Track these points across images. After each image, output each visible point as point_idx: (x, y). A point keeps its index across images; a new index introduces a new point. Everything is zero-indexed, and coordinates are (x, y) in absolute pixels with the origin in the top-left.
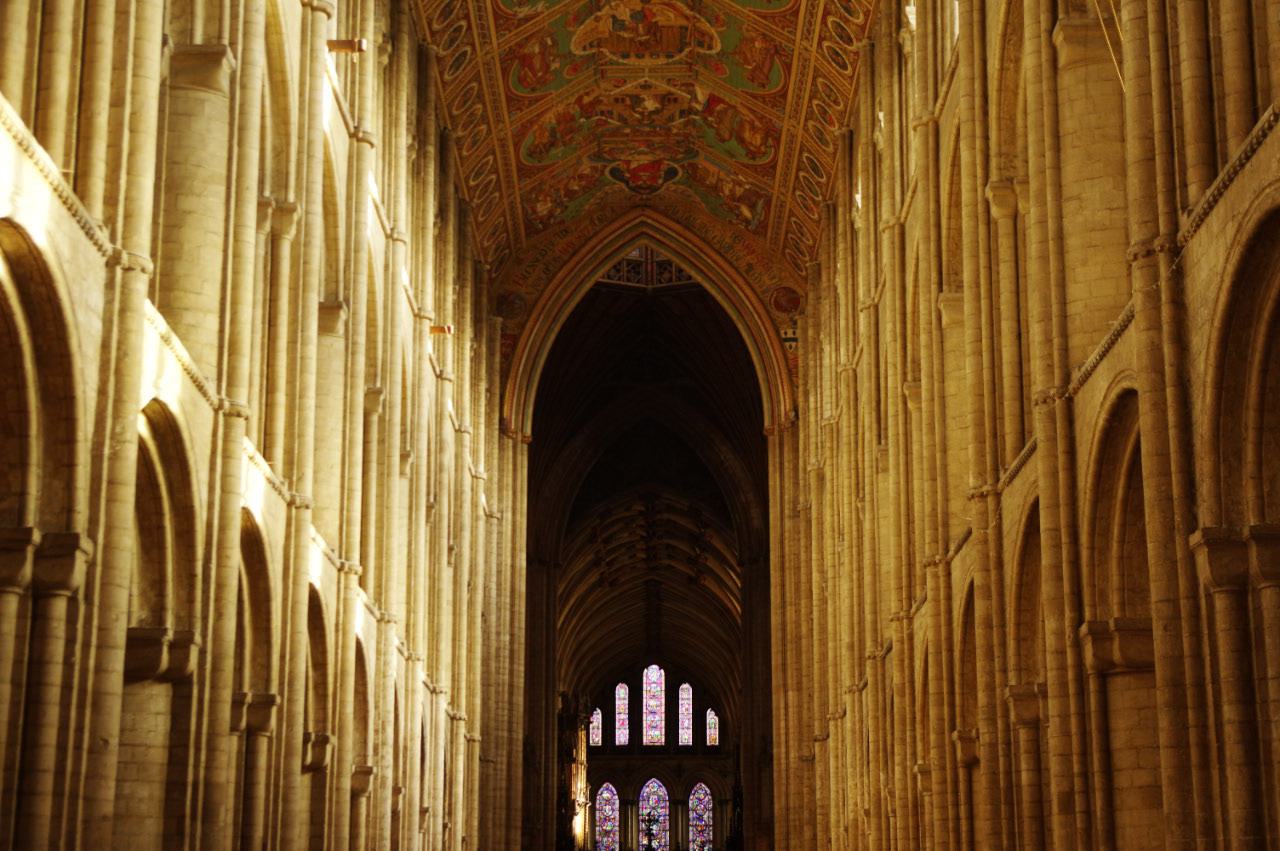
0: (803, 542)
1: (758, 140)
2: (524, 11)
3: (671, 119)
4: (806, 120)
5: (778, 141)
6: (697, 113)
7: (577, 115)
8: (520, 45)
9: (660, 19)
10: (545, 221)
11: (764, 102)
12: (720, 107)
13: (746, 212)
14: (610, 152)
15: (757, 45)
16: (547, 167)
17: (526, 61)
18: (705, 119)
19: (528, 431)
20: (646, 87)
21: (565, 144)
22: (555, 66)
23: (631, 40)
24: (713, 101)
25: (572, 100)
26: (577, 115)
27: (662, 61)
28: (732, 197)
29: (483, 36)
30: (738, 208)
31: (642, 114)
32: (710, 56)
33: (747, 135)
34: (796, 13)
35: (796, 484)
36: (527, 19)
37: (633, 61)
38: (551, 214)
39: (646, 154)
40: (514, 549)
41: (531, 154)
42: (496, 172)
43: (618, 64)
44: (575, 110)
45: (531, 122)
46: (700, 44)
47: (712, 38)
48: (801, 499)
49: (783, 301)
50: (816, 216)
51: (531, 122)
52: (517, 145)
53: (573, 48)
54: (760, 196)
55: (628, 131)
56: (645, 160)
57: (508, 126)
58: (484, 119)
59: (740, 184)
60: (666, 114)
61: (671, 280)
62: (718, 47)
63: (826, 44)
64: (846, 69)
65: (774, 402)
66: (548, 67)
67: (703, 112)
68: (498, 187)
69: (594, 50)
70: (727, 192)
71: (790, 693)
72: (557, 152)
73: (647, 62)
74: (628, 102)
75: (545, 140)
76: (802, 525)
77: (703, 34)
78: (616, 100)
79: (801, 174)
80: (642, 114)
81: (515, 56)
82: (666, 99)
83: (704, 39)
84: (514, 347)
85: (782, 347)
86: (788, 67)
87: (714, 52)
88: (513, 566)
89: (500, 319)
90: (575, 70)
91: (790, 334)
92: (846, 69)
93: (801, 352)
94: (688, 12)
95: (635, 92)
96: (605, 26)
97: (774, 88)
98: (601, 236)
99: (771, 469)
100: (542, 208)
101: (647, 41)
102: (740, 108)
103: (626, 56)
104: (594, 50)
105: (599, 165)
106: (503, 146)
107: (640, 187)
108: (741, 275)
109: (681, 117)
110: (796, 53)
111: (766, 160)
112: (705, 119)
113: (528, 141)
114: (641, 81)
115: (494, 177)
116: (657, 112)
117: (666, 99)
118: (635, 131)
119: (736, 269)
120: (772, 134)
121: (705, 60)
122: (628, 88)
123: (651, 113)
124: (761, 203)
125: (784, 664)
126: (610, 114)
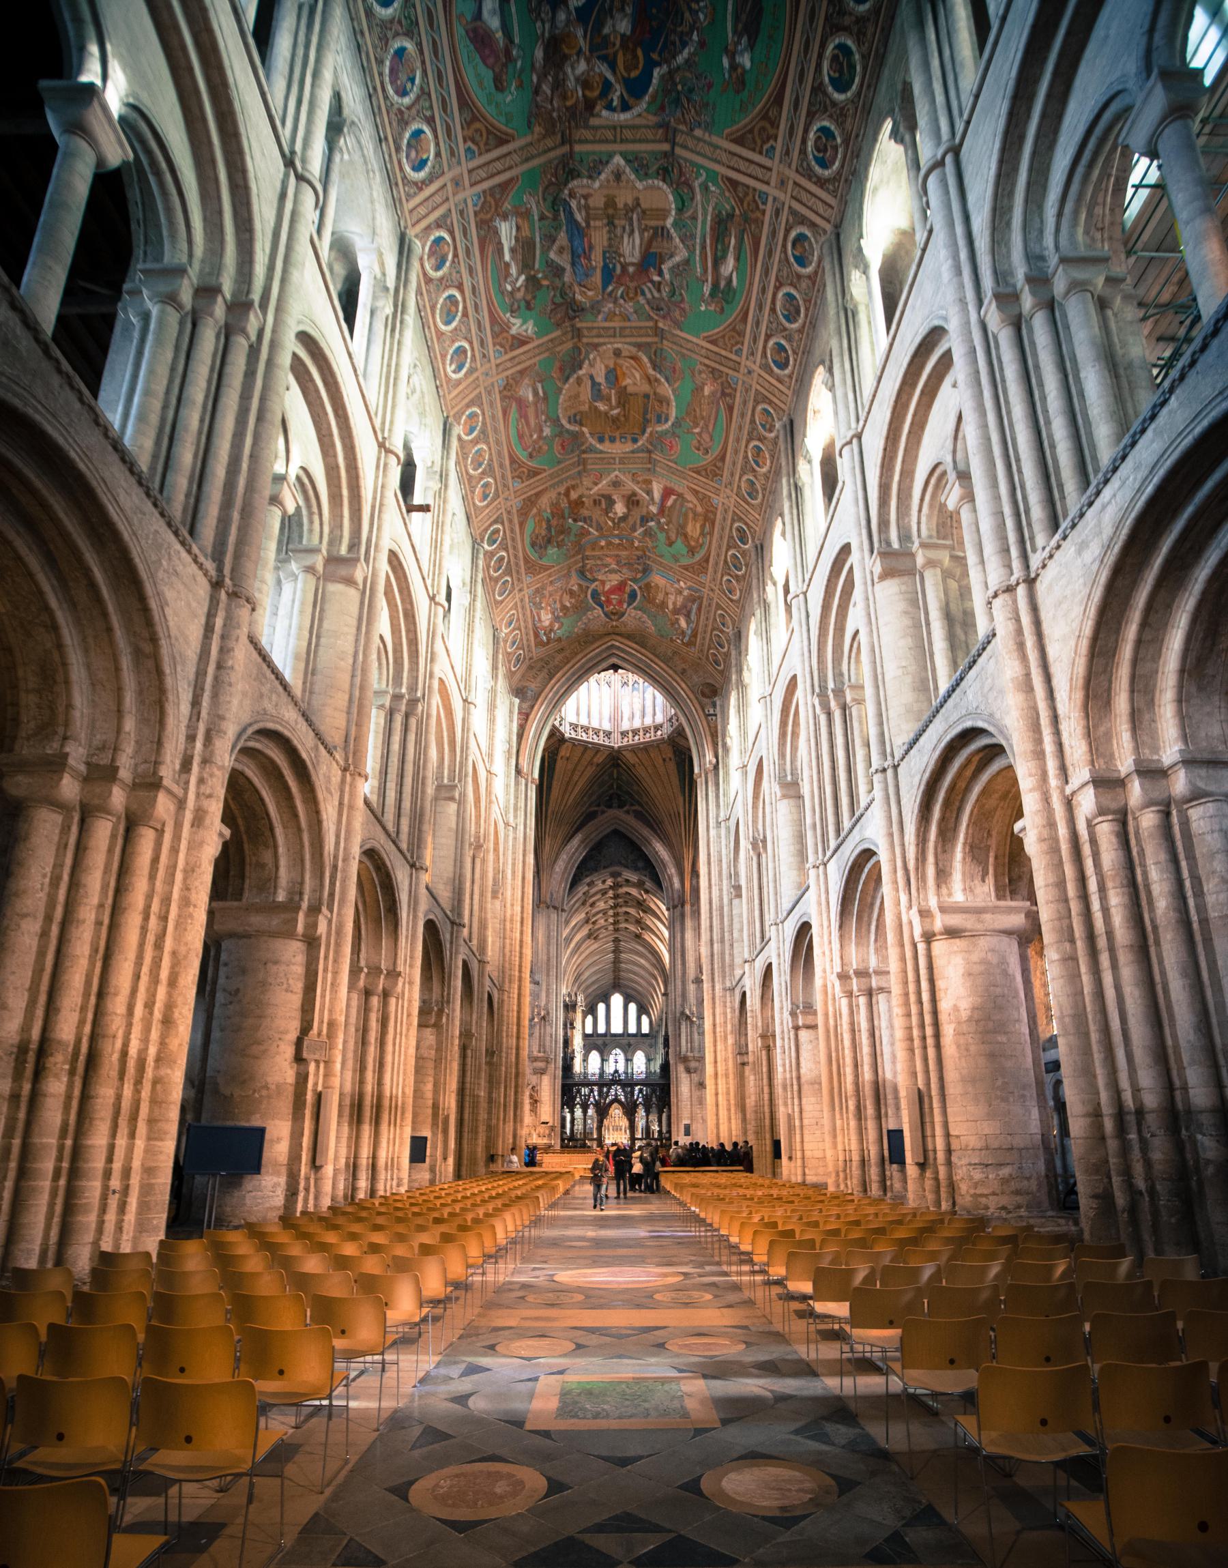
3: (634, 529)
7: (566, 512)
11: (707, 477)
12: (669, 503)
15: (707, 391)
18: (659, 522)
19: (536, 775)
20: (616, 484)
21: (559, 546)
23: (606, 414)
24: (667, 493)
25: (562, 490)
26: (566, 512)
27: (629, 447)
31: (613, 520)
32: (666, 432)
33: (689, 528)
37: (606, 447)
41: (533, 545)
44: (564, 504)
46: (659, 421)
49: (707, 691)
52: (522, 524)
54: (694, 601)
55: (603, 543)
60: (631, 520)
62: (673, 414)
66: (541, 431)
82: (632, 501)
89: (517, 701)
95: (610, 491)
96: (586, 392)
97: (715, 451)
103: (601, 440)
105: (584, 584)
106: (510, 521)
112: (659, 522)
116: (624, 518)
118: (609, 543)
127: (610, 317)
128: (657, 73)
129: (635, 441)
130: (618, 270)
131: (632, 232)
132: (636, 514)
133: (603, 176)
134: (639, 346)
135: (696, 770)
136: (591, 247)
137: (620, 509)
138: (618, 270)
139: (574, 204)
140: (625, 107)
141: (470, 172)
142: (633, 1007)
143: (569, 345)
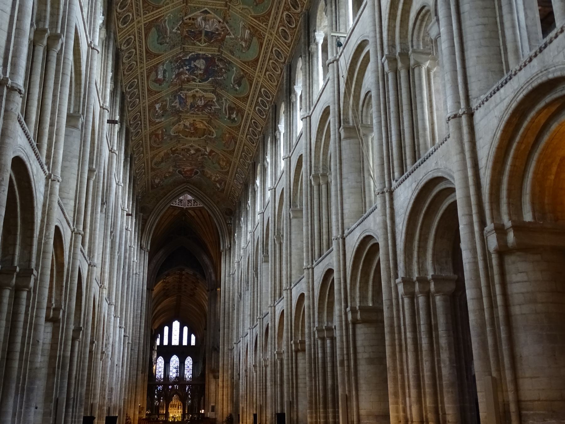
0: (231, 284)
1: (224, 164)
2: (158, 121)
3: (198, 156)
4: (240, 159)
5: (230, 165)
6: (206, 155)
8: (155, 131)
9: (198, 126)
10: (157, 185)
11: (227, 153)
12: (213, 154)
13: (218, 186)
14: (179, 165)
15: (227, 135)
16: (160, 169)
17: (157, 136)
19: (149, 248)
20: (192, 146)
21: (166, 162)
22: (165, 138)
23: (189, 132)
24: (211, 151)
27: (197, 139)
28: (215, 181)
29: (145, 127)
30: (216, 184)
31: (189, 154)
33: (221, 162)
34: (240, 127)
35: (230, 267)
36: (159, 123)
37: (189, 138)
38: (159, 182)
39: (189, 166)
40: (143, 284)
41: (155, 164)
42: (144, 169)
43: (184, 139)
45: (156, 155)
46: (209, 134)
47: (213, 133)
48: (231, 271)
50: (240, 188)
51: (156, 155)
52: (151, 161)
53: (171, 133)
54: (223, 181)
55: (185, 159)
56: (189, 168)
57: (149, 156)
58: (143, 152)
59: (218, 177)
60: (197, 155)
61: (191, 205)
63: (248, 136)
64: (254, 144)
65: (224, 242)
66: (163, 138)
67: (208, 155)
68: (144, 174)
69: (177, 134)
70: (213, 179)
71: (226, 330)
72: (163, 164)
73: (193, 139)
74: (186, 150)
75: (160, 160)
76: (231, 279)
77: (210, 131)
78: (182, 150)
79: (237, 175)
80: (189, 154)
81: (154, 134)
82: (197, 150)
83: (210, 133)
84: (146, 223)
85: (227, 226)
86: (236, 143)
87: (213, 137)
88: (142, 290)
89: (142, 214)
90: (171, 139)
91: (229, 222)
92: (254, 144)
93: (232, 227)
94: (207, 124)
95: (188, 148)
96: (182, 127)
98: (174, 190)
99: (222, 262)
100: (157, 181)
101: (193, 132)
102: (220, 154)
103: (186, 136)
104: (177, 134)
105: (175, 169)
107: (187, 177)
108: (215, 203)
109: (201, 156)
110: (239, 138)
111: (226, 170)
113: (155, 160)
114: (190, 144)
115: (144, 170)
116: (194, 154)
117: (197, 150)
119: (214, 202)
120: (229, 163)
121: (211, 139)
122: (186, 146)
123: (192, 154)
124: (223, 183)
125: (224, 321)
126: (180, 154)
127: (192, 114)
128: (210, 79)
129: (200, 138)
130: (196, 106)
131: (201, 100)
132: (199, 153)
133: (192, 91)
134: (203, 120)
135: (222, 248)
136: (186, 102)
137: (192, 152)
138: (196, 106)
139: (181, 95)
140: (200, 82)
141: (146, 69)
142: (186, 329)
143: (177, 119)
